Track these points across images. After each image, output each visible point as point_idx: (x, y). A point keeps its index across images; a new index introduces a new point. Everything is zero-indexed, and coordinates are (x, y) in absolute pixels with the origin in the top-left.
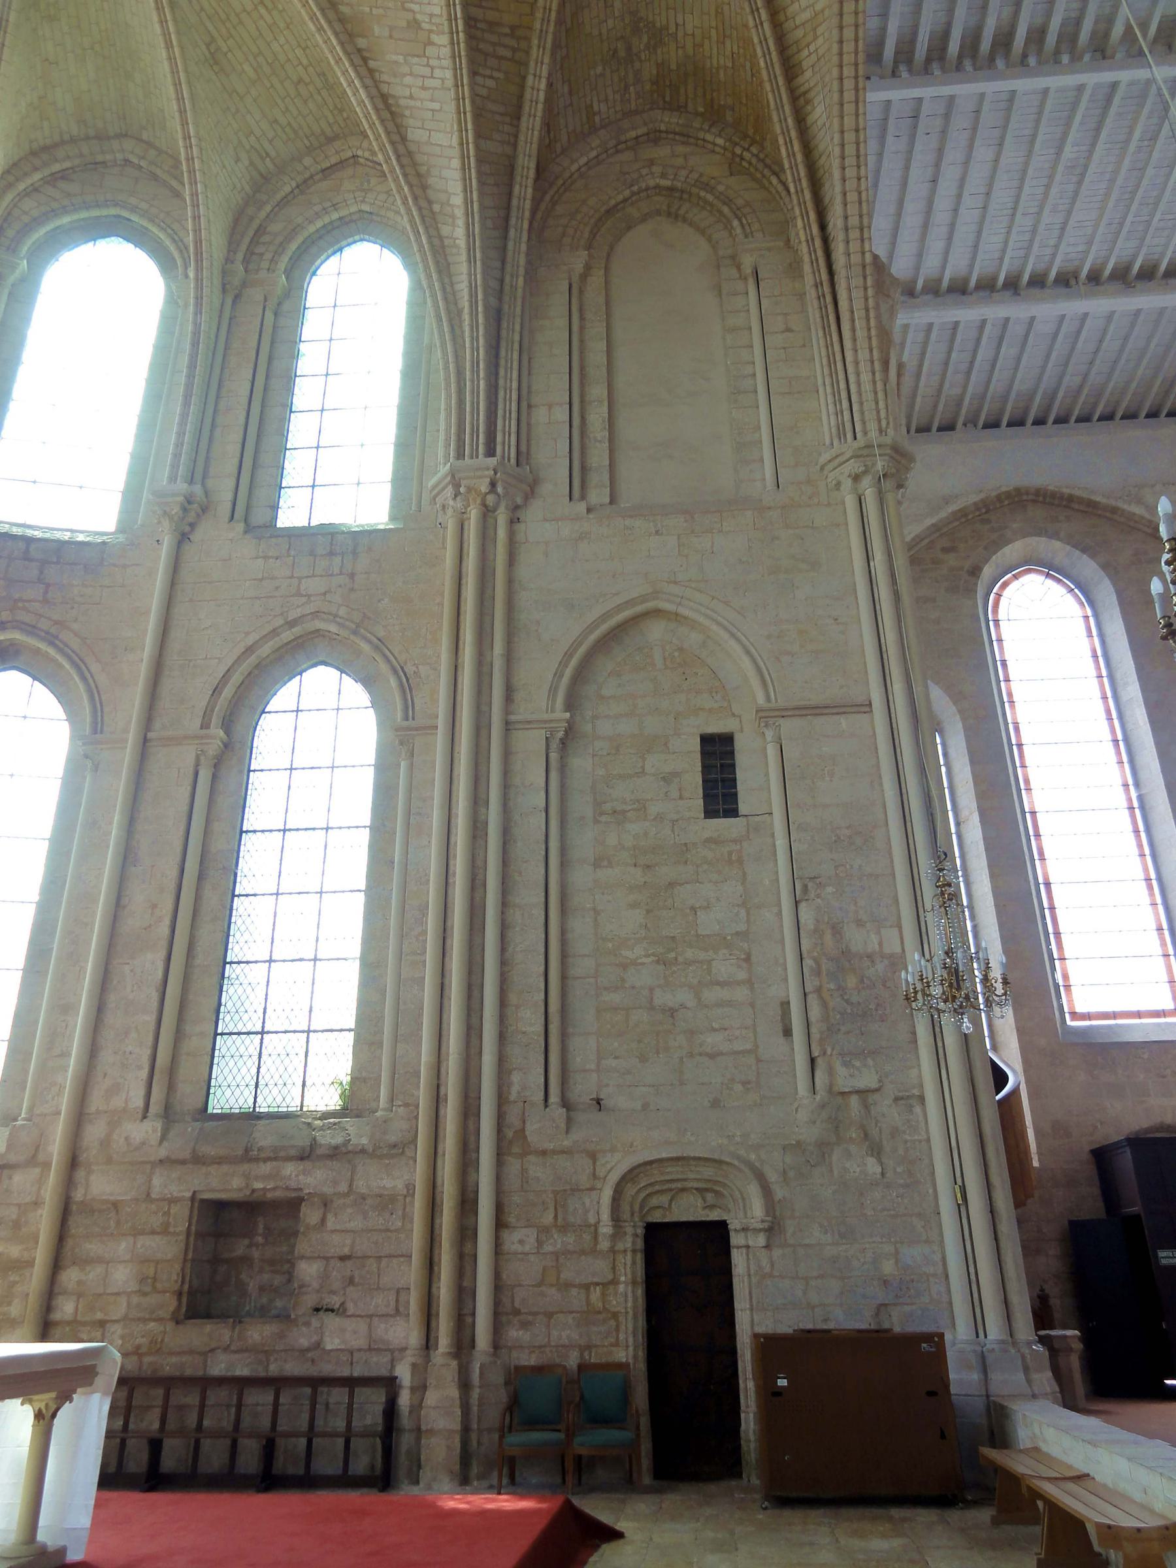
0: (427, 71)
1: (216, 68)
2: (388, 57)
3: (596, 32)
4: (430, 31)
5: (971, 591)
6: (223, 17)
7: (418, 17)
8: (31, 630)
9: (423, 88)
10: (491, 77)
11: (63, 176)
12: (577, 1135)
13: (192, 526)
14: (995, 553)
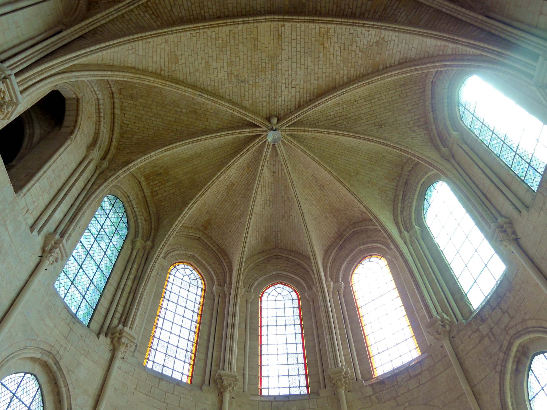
0: (392, 42)
2: (386, 58)
4: (380, 37)
6: (369, 116)
7: (375, 41)
8: (518, 335)
9: (398, 45)
10: (401, 13)
11: (404, 195)
13: (514, 233)
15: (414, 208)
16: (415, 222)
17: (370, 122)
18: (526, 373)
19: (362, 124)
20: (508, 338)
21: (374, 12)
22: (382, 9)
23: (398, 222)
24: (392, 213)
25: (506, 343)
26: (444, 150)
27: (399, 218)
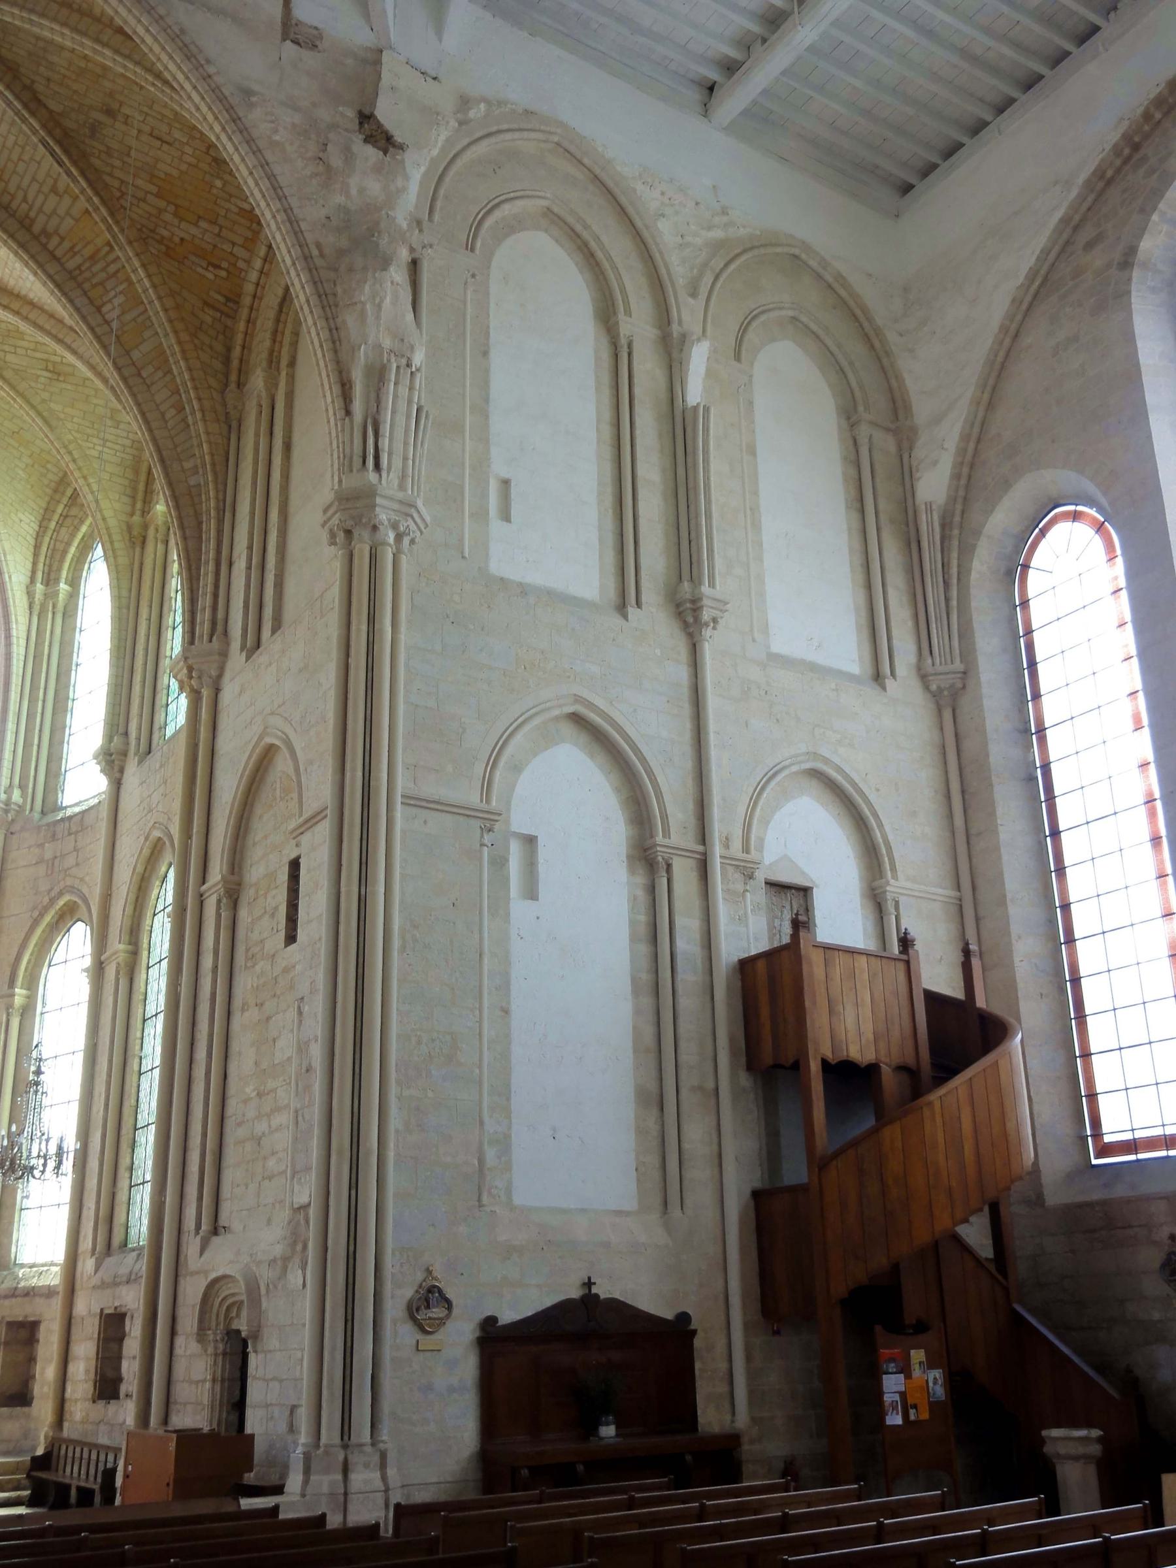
1: (61, 378)
3: (184, 167)
5: (1123, 296)
12: (202, 1259)
13: (122, 771)
14: (1155, 209)
15: (80, 536)
16: (69, 568)
17: (38, 355)
18: (62, 934)
19: (19, 351)
20: (62, 885)
21: (72, 248)
22: (87, 252)
23: (40, 547)
24: (40, 518)
25: (56, 890)
26: (137, 519)
27: (47, 539)
